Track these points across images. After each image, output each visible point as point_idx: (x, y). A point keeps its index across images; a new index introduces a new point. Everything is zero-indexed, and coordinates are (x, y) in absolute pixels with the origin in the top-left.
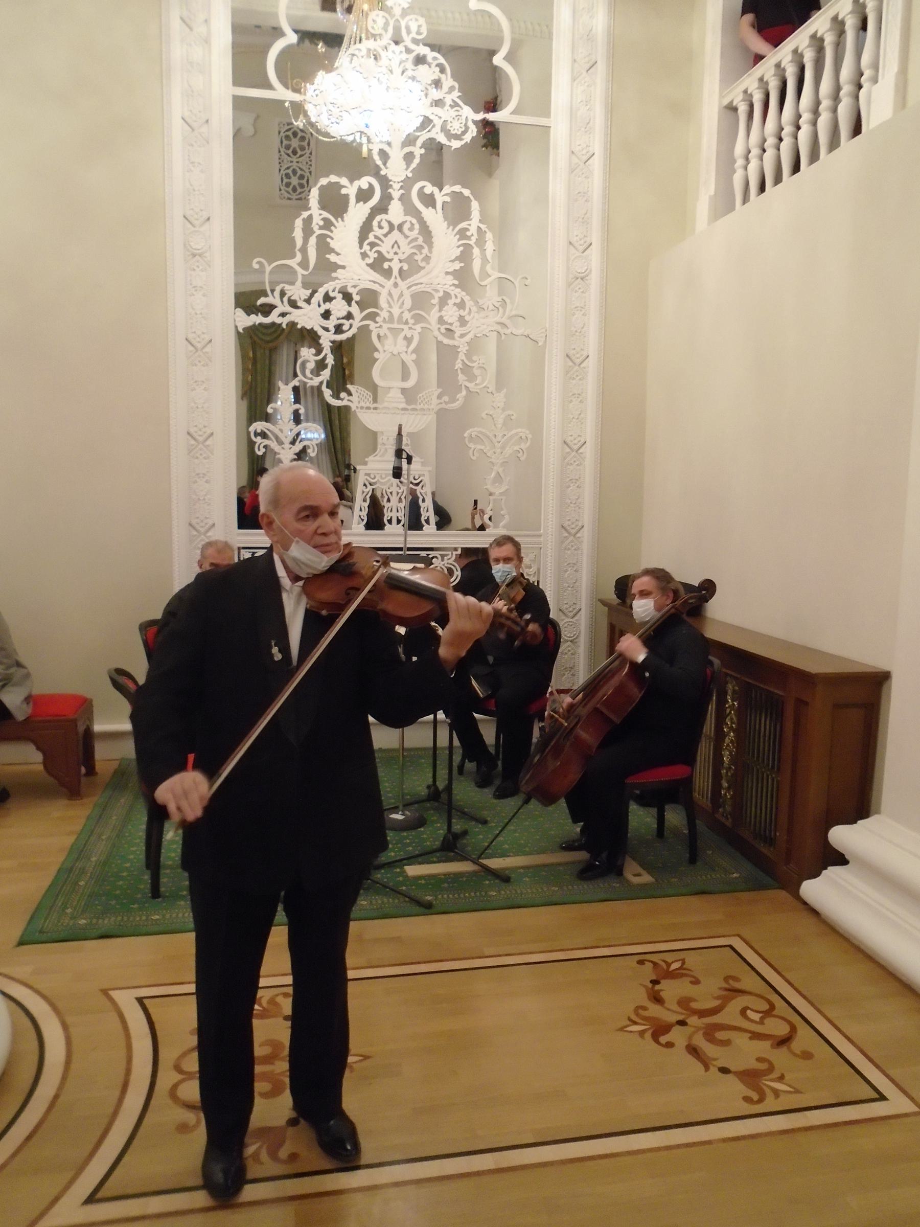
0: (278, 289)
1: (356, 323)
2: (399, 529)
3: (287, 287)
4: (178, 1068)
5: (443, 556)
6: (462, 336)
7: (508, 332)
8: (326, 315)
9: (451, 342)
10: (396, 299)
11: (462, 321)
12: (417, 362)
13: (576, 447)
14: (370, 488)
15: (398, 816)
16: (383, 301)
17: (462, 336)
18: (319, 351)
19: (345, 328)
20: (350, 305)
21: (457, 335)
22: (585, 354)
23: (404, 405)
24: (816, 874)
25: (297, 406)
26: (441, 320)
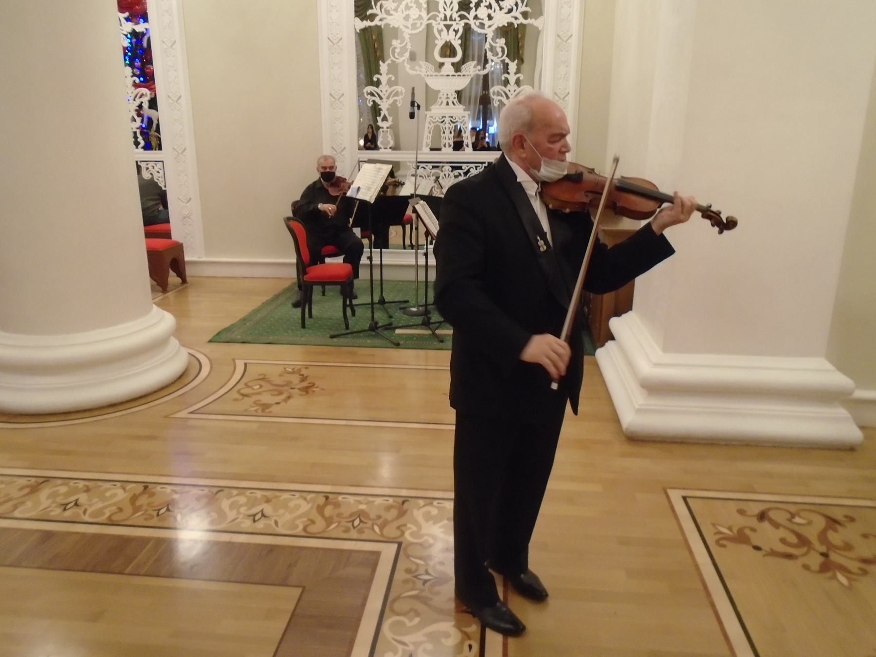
0: (379, 4)
1: (425, 22)
2: (451, 149)
3: (384, 2)
4: (246, 384)
5: (476, 167)
6: (490, 27)
7: (519, 22)
8: (407, 18)
9: (482, 31)
10: (448, 4)
11: (490, 17)
12: (461, 45)
13: (562, 97)
14: (433, 125)
15: (414, 309)
16: (441, 10)
17: (490, 27)
18: (403, 40)
19: (418, 25)
20: (420, 11)
21: (486, 27)
22: (570, 34)
23: (454, 73)
24: (602, 345)
25: (390, 76)
26: (476, 17)
